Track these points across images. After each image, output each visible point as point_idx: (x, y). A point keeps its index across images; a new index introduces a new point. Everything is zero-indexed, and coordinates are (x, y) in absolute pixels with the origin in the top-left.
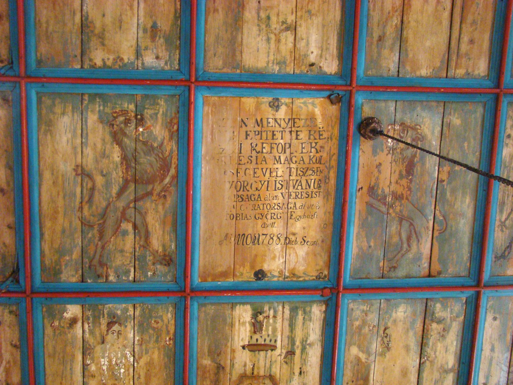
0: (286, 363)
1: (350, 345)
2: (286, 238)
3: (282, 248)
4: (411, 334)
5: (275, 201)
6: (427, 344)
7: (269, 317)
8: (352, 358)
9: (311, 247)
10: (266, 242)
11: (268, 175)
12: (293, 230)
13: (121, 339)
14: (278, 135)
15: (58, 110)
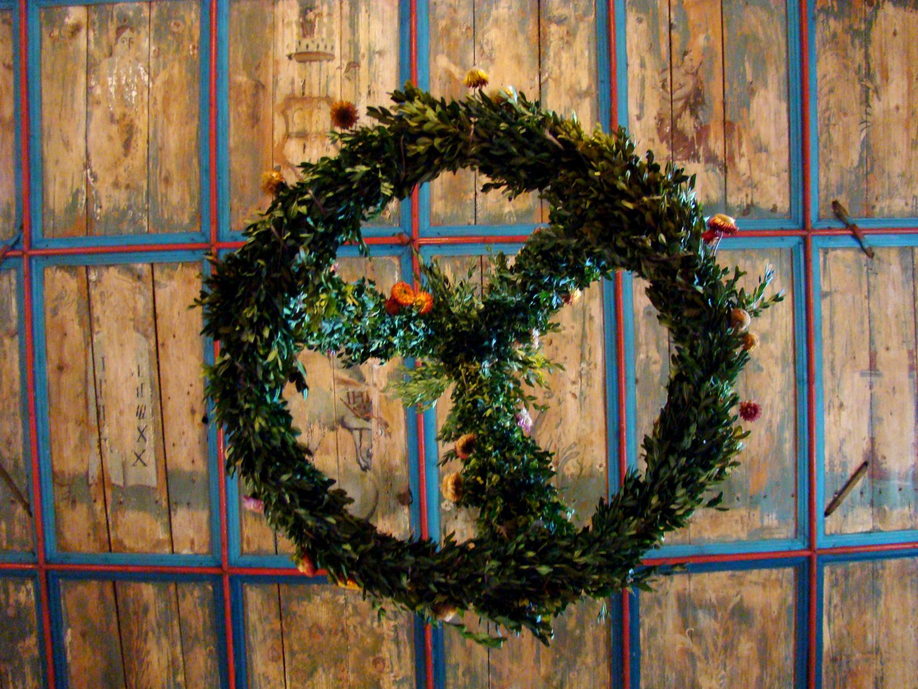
0: (349, 79)
1: (436, 54)
4: (521, 38)
6: (546, 54)
7: (321, 14)
8: (440, 72)
13: (133, 50)
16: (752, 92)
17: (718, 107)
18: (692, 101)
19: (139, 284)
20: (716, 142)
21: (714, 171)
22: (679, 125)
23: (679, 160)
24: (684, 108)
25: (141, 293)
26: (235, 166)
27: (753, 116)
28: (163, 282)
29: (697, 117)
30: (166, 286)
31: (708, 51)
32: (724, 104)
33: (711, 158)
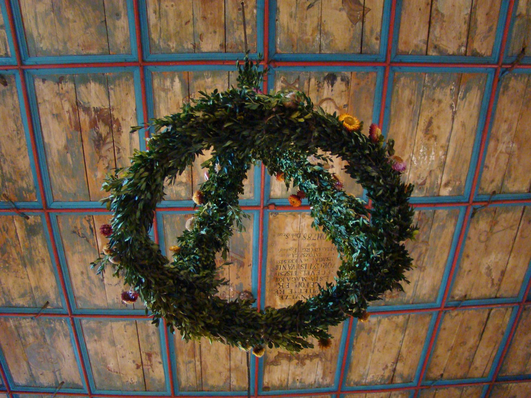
2: (300, 237)
3: (302, 231)
5: (306, 258)
9: (282, 232)
10: (313, 236)
11: (311, 272)
12: (294, 242)
13: (419, 173)
14: (303, 291)
15: (427, 296)
16: (66, 148)
17: (85, 139)
18: (101, 142)
19: (436, 43)
20: (85, 119)
21: (84, 103)
22: (108, 128)
23: (106, 109)
24: (106, 138)
25: (436, 38)
26: (370, 109)
27: (64, 135)
28: (422, 44)
29: (97, 133)
30: (420, 41)
31: (95, 169)
32: (82, 141)
33: (87, 110)
